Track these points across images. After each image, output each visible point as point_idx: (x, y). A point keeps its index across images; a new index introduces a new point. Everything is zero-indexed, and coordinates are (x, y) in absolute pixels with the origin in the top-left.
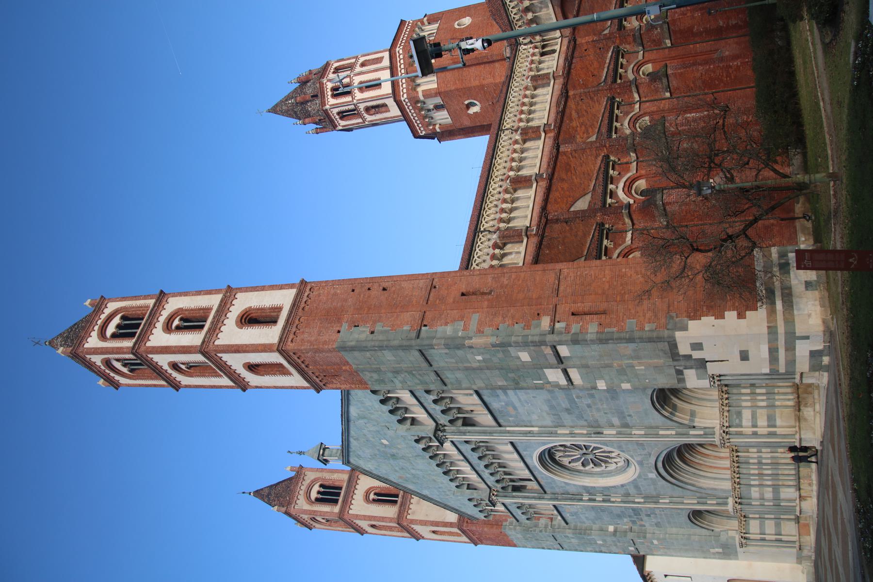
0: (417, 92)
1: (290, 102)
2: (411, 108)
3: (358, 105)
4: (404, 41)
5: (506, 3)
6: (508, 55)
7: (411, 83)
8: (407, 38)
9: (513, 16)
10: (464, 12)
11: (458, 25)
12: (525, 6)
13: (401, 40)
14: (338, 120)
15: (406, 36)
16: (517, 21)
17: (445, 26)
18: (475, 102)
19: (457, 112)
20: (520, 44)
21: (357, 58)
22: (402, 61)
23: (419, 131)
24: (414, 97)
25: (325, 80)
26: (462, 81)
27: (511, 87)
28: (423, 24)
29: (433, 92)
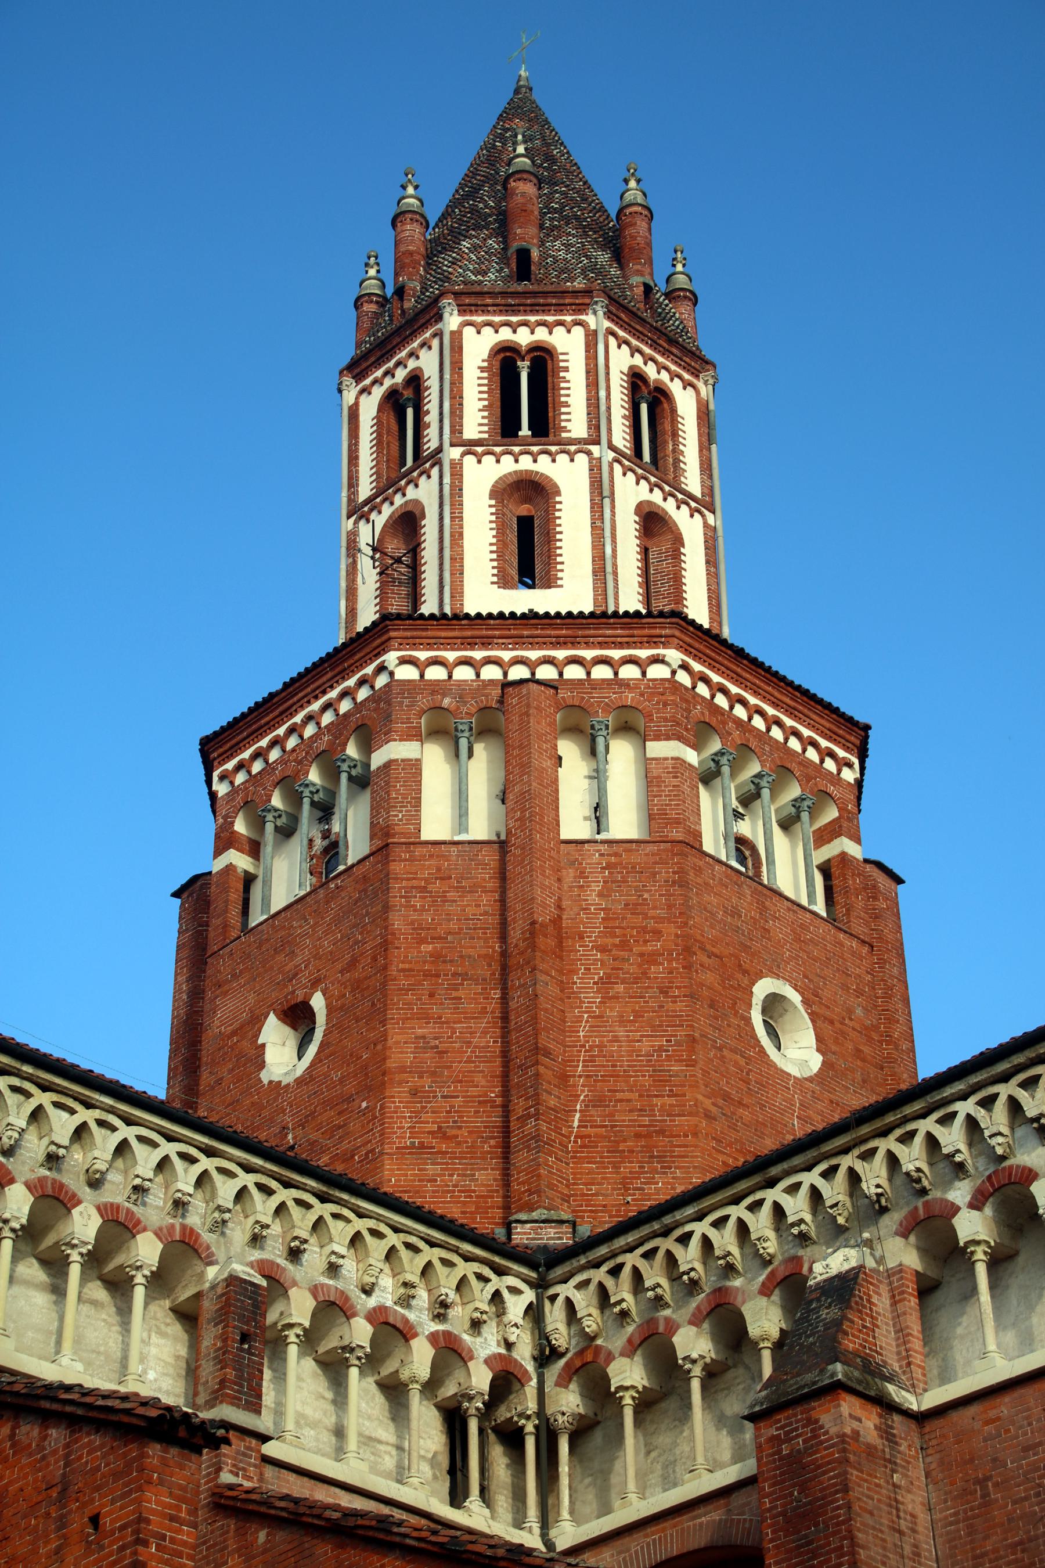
0: (413, 735)
1: (521, 149)
2: (345, 706)
3: (435, 472)
4: (721, 701)
5: (771, 1183)
6: (516, 1239)
7: (472, 706)
8: (745, 726)
9: (700, 1228)
10: (858, 1053)
11: (773, 1004)
12: (747, 1311)
13: (734, 689)
14: (388, 382)
15: (758, 722)
16: (669, 1254)
17: (780, 931)
18: (312, 1050)
19: (280, 958)
20: (540, 1285)
21: (704, 504)
22: (602, 672)
23: (230, 765)
24: (388, 718)
25: (596, 320)
26: (427, 975)
27: (210, 1153)
28: (824, 836)
29: (398, 816)
